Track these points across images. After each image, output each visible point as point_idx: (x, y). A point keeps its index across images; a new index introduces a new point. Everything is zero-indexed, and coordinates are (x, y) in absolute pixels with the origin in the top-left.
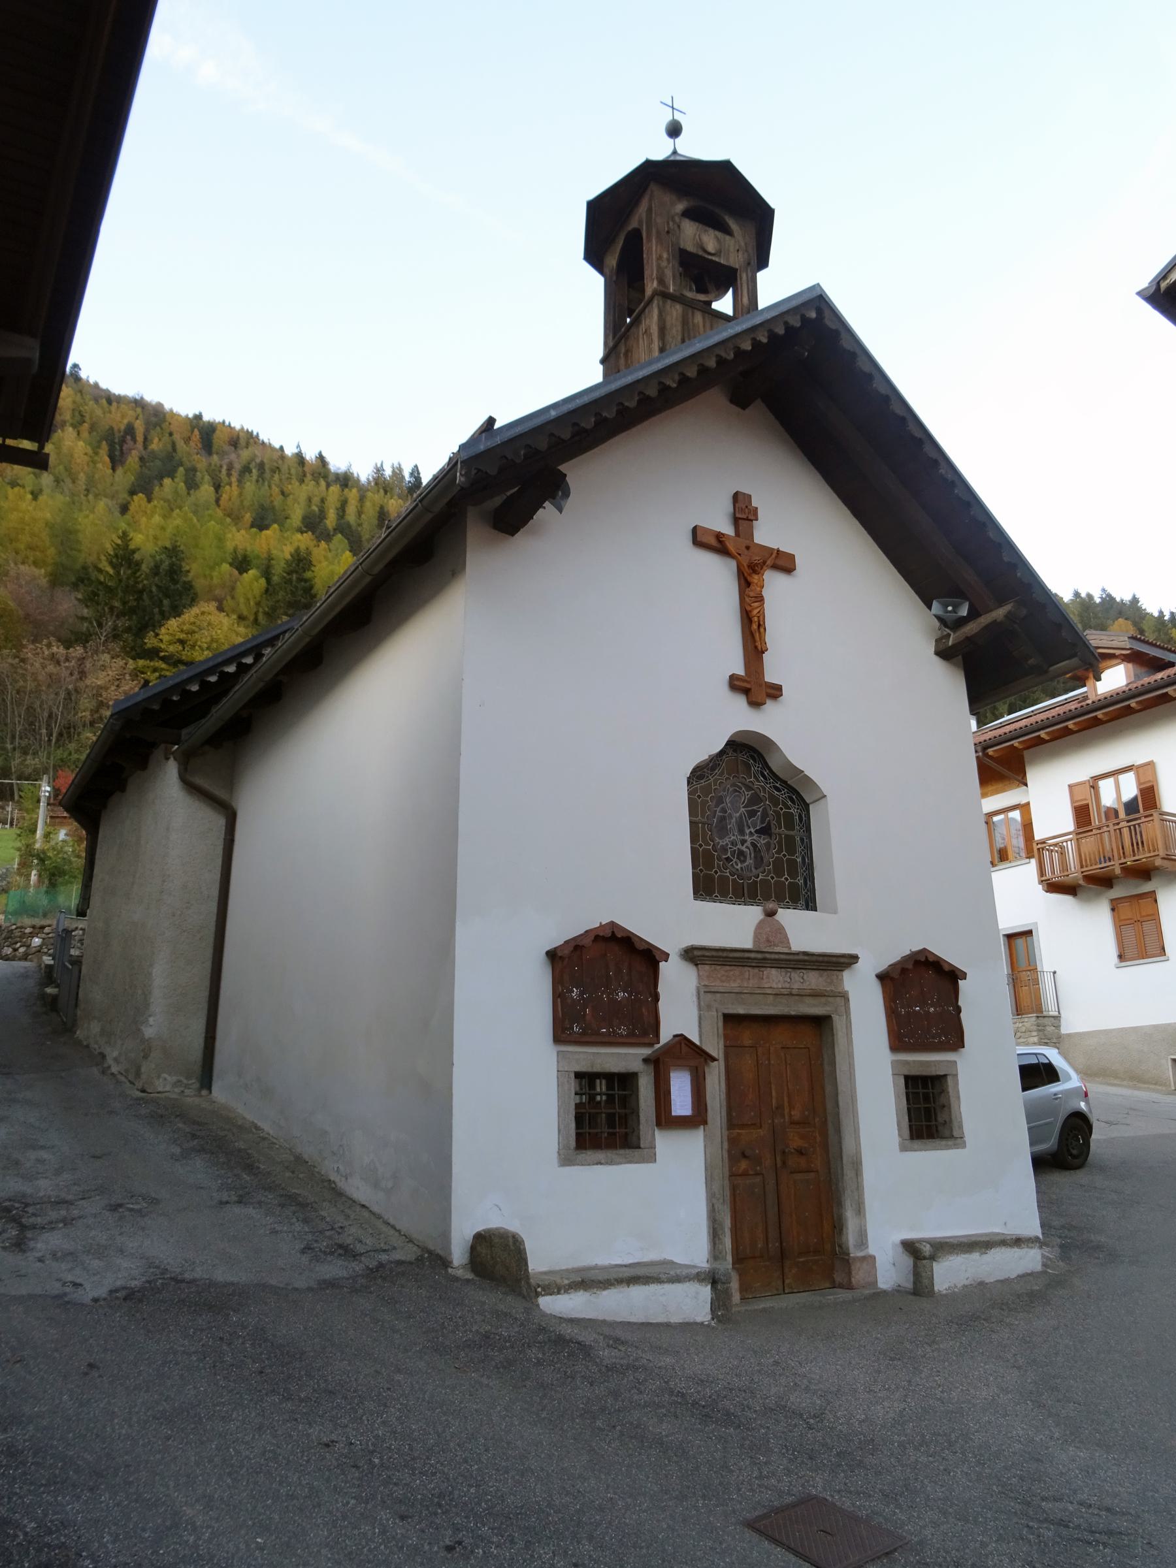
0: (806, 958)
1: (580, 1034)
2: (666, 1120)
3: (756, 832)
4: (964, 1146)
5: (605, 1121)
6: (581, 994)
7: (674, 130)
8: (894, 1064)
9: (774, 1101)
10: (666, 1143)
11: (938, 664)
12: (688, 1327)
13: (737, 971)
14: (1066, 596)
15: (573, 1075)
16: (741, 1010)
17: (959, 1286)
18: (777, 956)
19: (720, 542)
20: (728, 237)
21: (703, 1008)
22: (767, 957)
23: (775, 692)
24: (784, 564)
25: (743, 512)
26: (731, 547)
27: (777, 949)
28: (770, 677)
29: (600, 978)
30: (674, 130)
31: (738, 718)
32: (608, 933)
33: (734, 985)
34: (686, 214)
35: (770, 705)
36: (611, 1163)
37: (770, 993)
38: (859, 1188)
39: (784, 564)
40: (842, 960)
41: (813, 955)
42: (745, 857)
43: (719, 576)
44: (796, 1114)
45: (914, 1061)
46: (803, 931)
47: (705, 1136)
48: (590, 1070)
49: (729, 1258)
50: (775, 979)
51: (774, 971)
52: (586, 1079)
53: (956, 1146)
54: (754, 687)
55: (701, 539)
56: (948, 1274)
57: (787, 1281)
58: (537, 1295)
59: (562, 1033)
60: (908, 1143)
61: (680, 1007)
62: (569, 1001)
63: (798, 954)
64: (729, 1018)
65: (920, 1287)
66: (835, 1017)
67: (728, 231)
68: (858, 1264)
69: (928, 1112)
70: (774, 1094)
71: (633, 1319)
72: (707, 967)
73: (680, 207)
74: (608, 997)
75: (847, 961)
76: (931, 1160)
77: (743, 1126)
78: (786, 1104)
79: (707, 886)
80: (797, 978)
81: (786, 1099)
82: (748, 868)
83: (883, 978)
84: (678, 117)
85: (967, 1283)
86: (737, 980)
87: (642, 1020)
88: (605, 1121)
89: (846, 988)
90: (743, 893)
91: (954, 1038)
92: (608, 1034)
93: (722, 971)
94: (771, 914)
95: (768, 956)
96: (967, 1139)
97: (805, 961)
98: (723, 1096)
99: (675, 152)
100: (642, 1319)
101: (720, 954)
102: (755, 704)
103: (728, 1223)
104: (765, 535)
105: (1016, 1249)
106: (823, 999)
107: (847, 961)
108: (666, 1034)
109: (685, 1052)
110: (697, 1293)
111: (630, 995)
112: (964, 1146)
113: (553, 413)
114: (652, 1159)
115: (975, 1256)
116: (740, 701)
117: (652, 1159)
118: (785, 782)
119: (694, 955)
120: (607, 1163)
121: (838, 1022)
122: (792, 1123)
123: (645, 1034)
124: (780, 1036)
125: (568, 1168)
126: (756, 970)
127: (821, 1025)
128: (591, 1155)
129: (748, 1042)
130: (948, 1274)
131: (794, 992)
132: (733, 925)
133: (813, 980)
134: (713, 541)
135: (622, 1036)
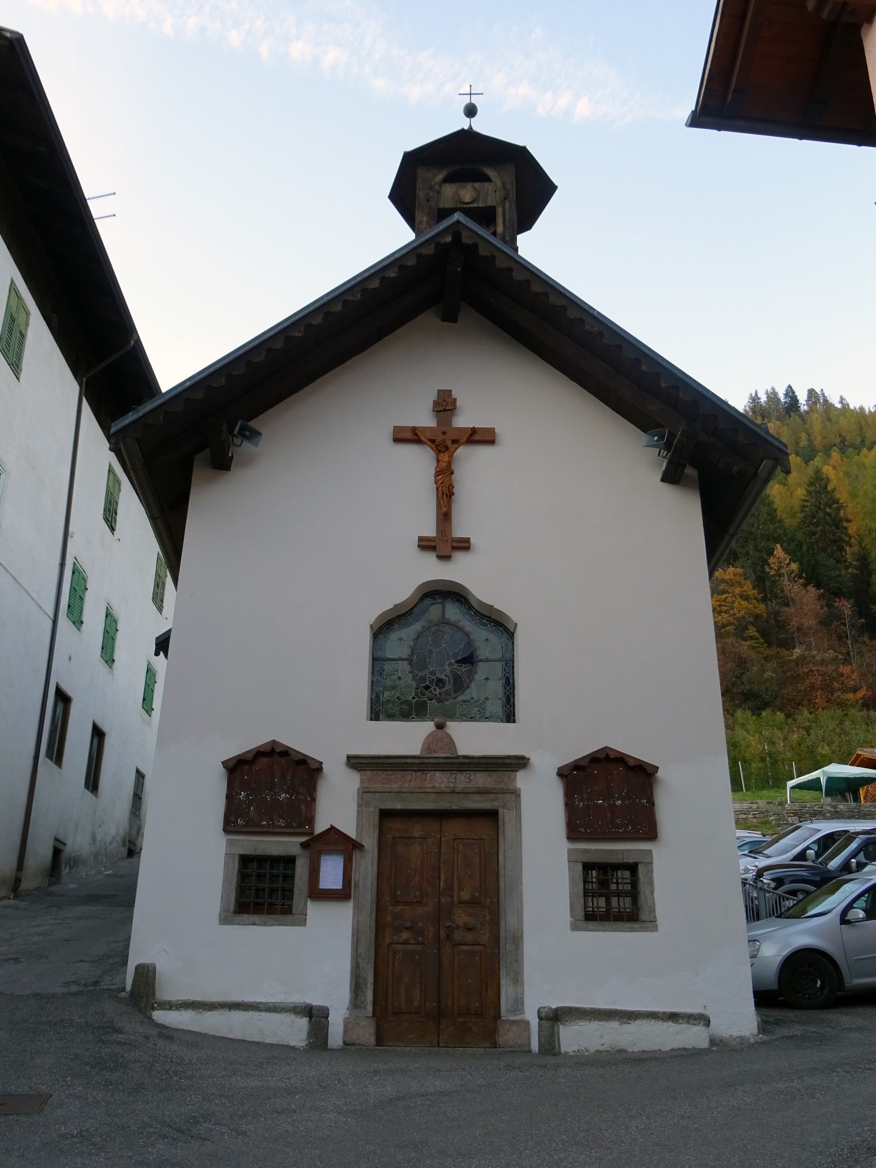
0: (467, 761)
1: (243, 826)
2: (318, 894)
3: (457, 662)
4: (655, 929)
5: (262, 891)
6: (248, 795)
7: (471, 111)
8: (570, 851)
9: (442, 884)
10: (315, 911)
11: (667, 489)
12: (293, 1048)
13: (399, 775)
14: (739, 402)
15: (237, 858)
16: (399, 806)
17: (592, 1050)
18: (435, 761)
19: (416, 434)
20: (486, 184)
21: (362, 804)
22: (441, 761)
23: (464, 545)
24: (482, 437)
25: (445, 405)
26: (423, 438)
27: (436, 755)
28: (459, 531)
29: (268, 784)
30: (471, 111)
31: (432, 570)
32: (269, 748)
33: (395, 786)
34: (447, 180)
35: (460, 557)
36: (265, 924)
37: (435, 790)
38: (518, 960)
39: (482, 437)
40: (508, 761)
41: (473, 758)
42: (444, 684)
43: (420, 461)
44: (465, 895)
45: (596, 850)
46: (473, 738)
47: (354, 907)
48: (253, 853)
49: (370, 1008)
50: (440, 780)
51: (438, 774)
52: (245, 860)
53: (645, 929)
54: (444, 543)
55: (407, 436)
56: (573, 1038)
57: (442, 1037)
58: (153, 1009)
59: (230, 826)
60: (582, 923)
61: (338, 805)
62: (237, 801)
63: (465, 757)
64: (385, 815)
65: (550, 1046)
66: (501, 811)
67: (488, 179)
68: (508, 1026)
69: (612, 896)
70: (442, 877)
71: (231, 1036)
72: (369, 773)
73: (440, 177)
74: (271, 798)
75: (520, 763)
76: (611, 942)
77: (406, 904)
78: (456, 886)
79: (379, 710)
80: (463, 778)
81: (456, 882)
82: (448, 693)
83: (564, 773)
84: (475, 100)
85: (602, 1048)
86: (397, 781)
87: (299, 814)
88: (262, 891)
89: (518, 786)
90: (410, 711)
91: (646, 828)
92: (268, 826)
93: (383, 775)
94: (440, 726)
95: (426, 761)
96: (659, 922)
97: (466, 764)
98: (375, 875)
99: (470, 127)
100: (257, 1039)
101: (376, 761)
102: (444, 558)
103: (370, 979)
104: (463, 421)
105: (670, 1023)
106: (492, 796)
107: (520, 763)
108: (320, 827)
109: (336, 841)
110: (293, 1022)
111: (291, 796)
112: (655, 929)
113: (188, 384)
114: (303, 923)
115: (614, 1024)
116: (430, 558)
117: (303, 923)
118: (490, 617)
119: (356, 763)
120: (260, 924)
121: (506, 816)
122: (460, 903)
123: (302, 825)
124: (453, 829)
125: (227, 926)
126: (419, 774)
127: (492, 815)
128: (245, 917)
129: (416, 835)
130: (573, 1038)
131: (457, 790)
132: (407, 738)
133: (481, 779)
134: (409, 435)
135: (280, 827)
